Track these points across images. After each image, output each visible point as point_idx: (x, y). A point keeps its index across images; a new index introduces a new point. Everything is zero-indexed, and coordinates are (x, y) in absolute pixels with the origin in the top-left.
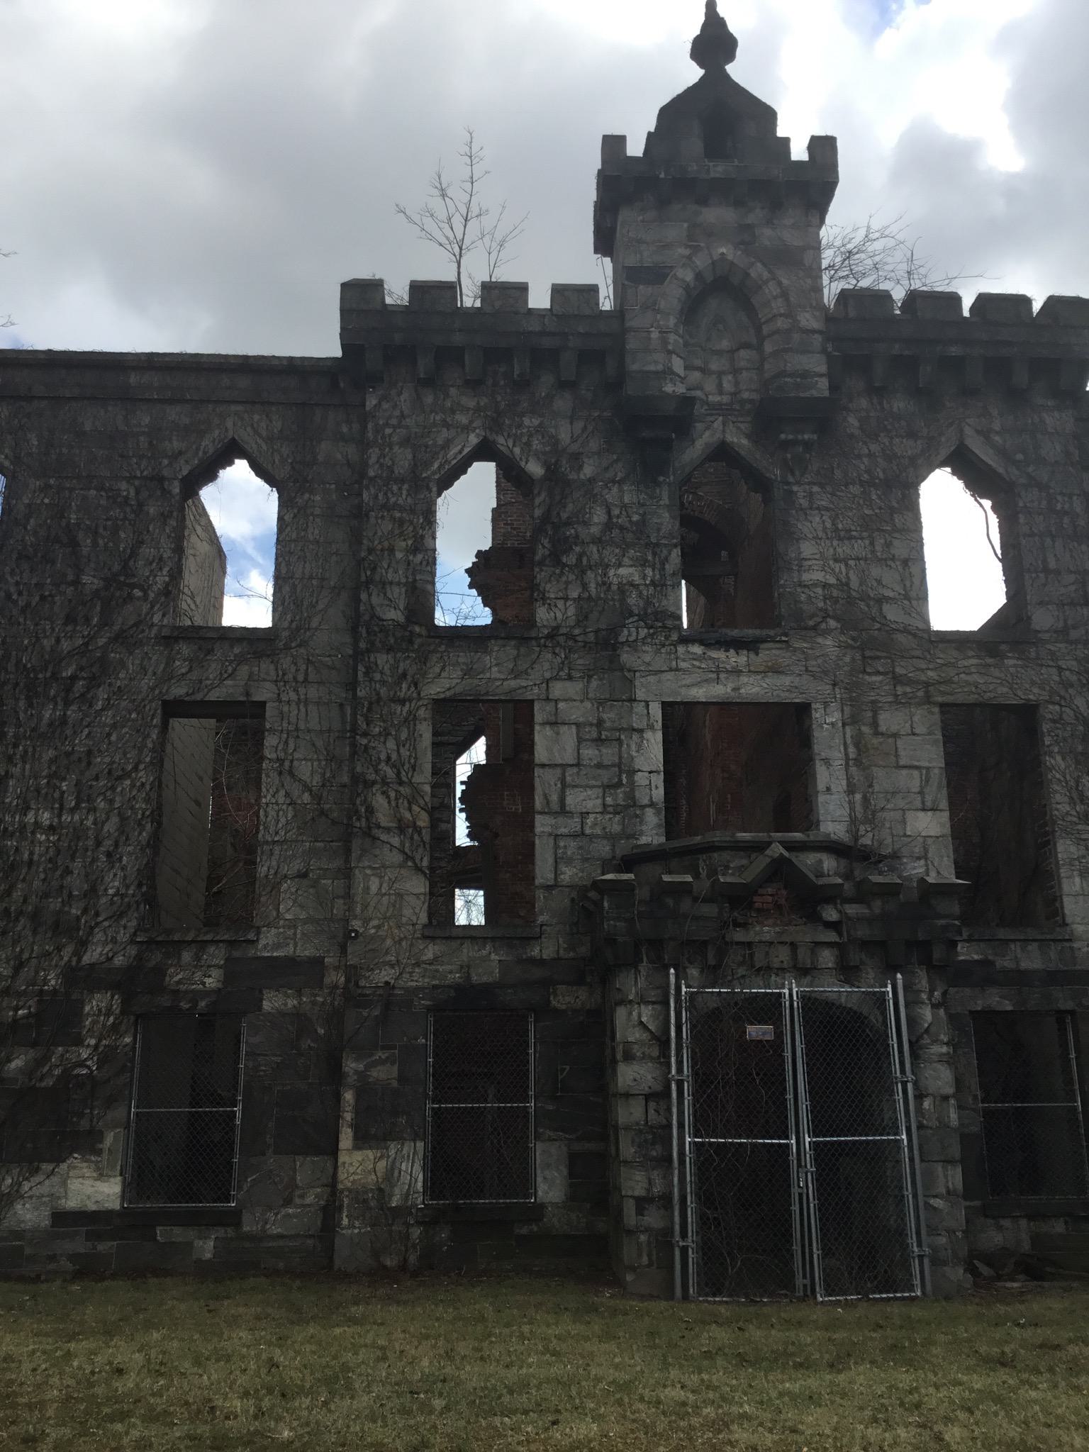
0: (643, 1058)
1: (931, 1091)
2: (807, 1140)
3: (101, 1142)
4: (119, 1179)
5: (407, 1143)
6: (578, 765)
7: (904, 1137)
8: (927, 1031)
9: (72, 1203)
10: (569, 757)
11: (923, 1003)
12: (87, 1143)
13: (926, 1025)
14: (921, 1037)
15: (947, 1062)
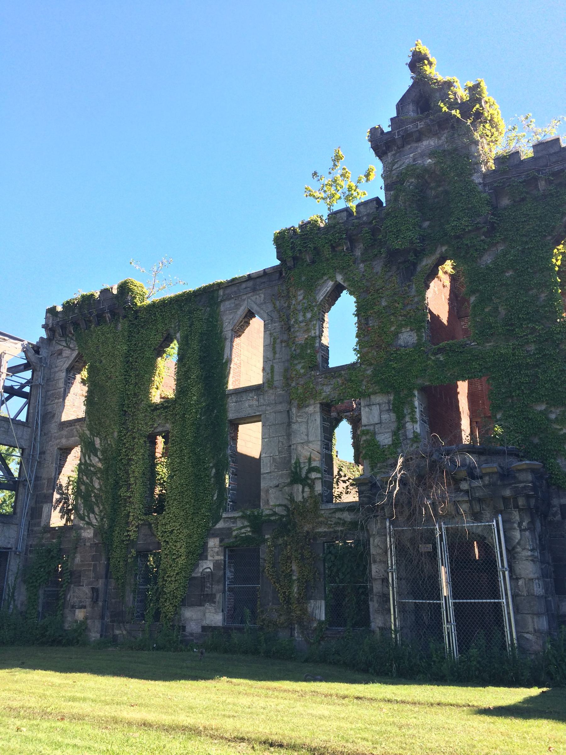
0: (380, 562)
1: (522, 576)
2: (450, 601)
3: (215, 598)
4: (221, 613)
5: (318, 601)
6: (380, 423)
7: (504, 601)
8: (518, 543)
9: (206, 623)
10: (376, 420)
11: (515, 529)
12: (210, 599)
13: (517, 541)
14: (514, 548)
15: (532, 560)
